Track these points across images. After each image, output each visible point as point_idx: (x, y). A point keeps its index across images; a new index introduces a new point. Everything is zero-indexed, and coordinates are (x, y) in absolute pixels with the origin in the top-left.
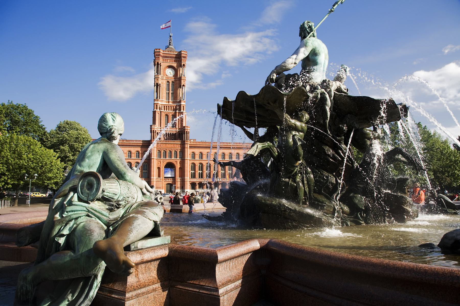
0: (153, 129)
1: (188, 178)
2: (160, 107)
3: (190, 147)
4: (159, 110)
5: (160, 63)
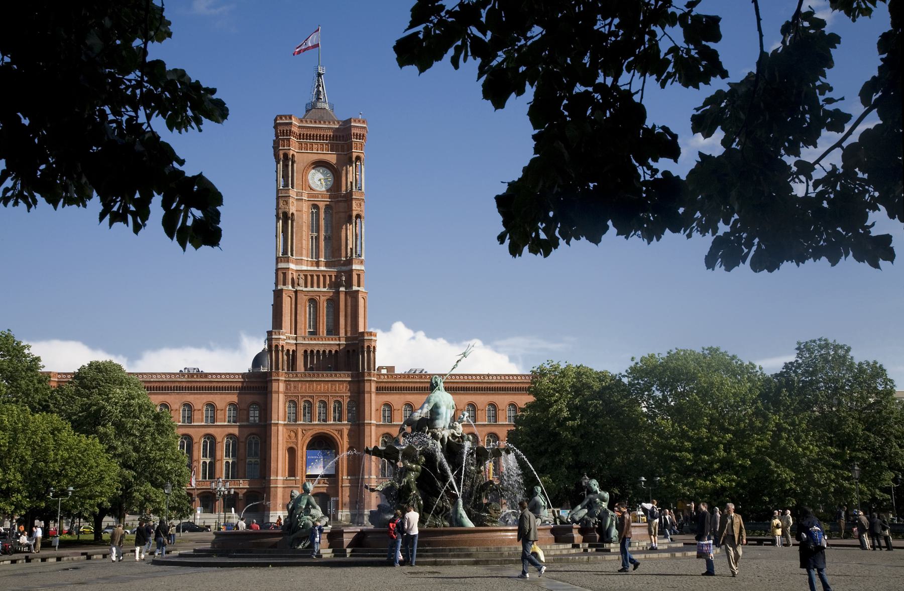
0: (274, 343)
1: (373, 477)
2: (293, 279)
3: (378, 389)
4: (290, 287)
5: (293, 155)
